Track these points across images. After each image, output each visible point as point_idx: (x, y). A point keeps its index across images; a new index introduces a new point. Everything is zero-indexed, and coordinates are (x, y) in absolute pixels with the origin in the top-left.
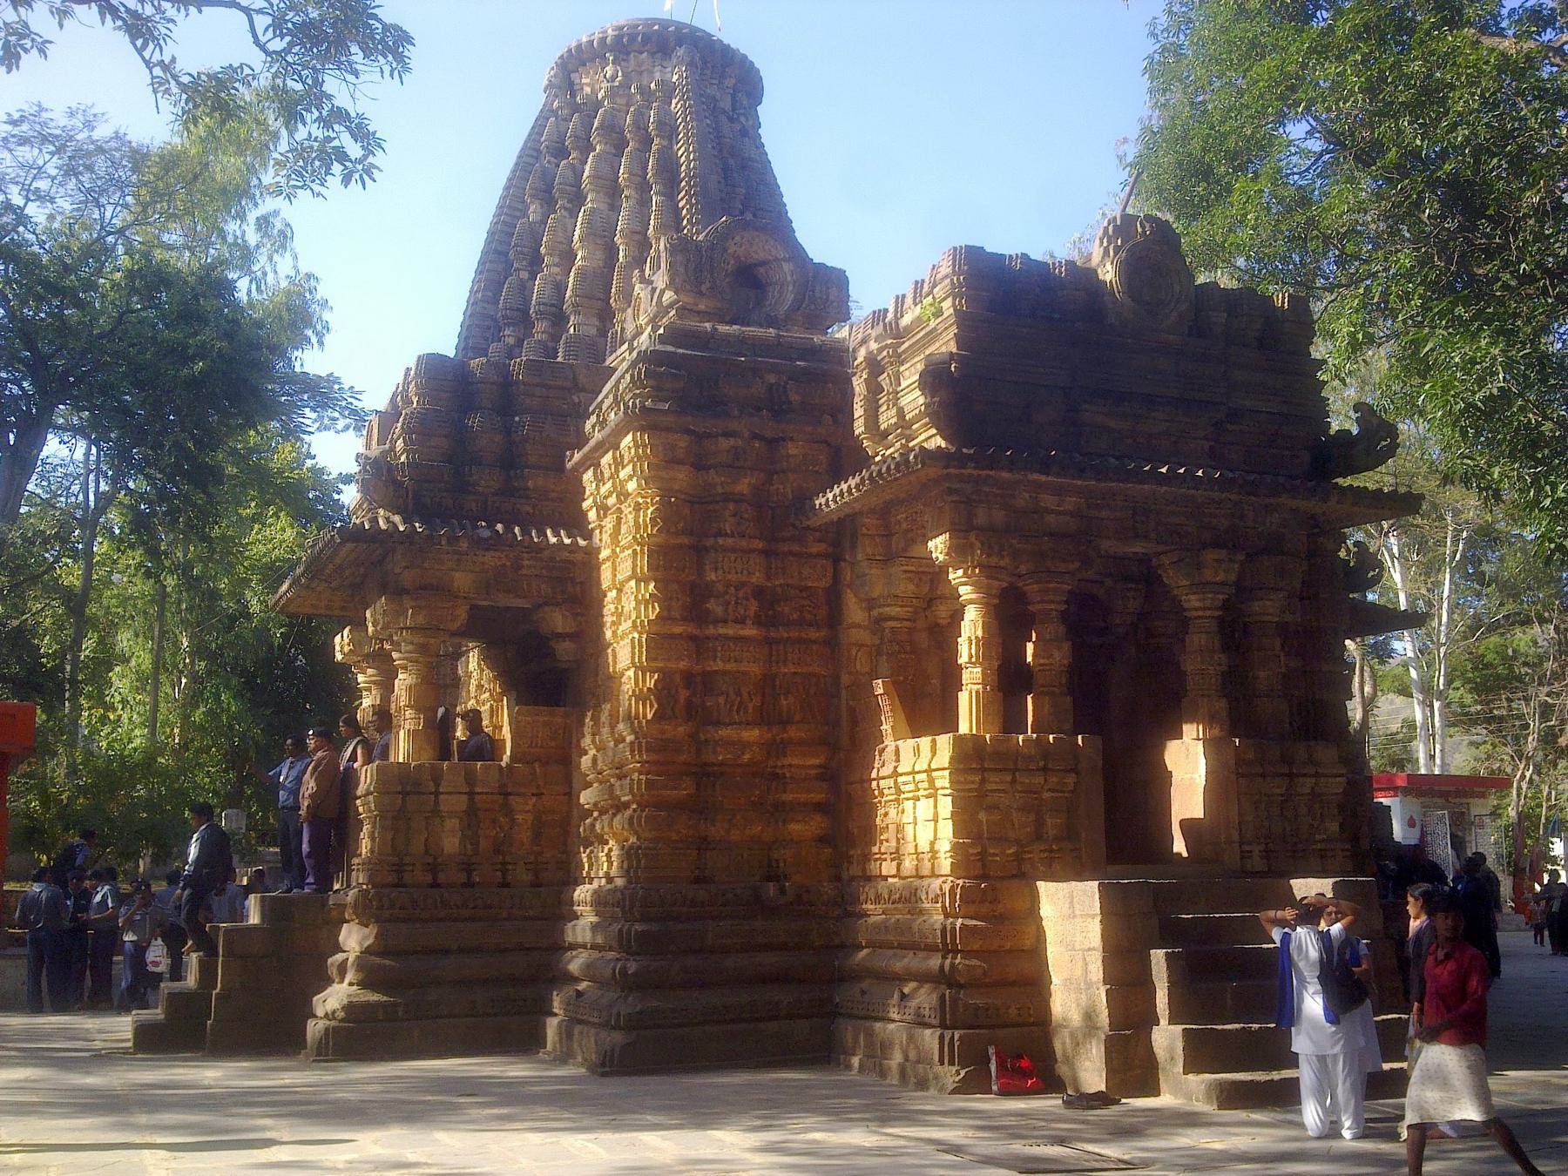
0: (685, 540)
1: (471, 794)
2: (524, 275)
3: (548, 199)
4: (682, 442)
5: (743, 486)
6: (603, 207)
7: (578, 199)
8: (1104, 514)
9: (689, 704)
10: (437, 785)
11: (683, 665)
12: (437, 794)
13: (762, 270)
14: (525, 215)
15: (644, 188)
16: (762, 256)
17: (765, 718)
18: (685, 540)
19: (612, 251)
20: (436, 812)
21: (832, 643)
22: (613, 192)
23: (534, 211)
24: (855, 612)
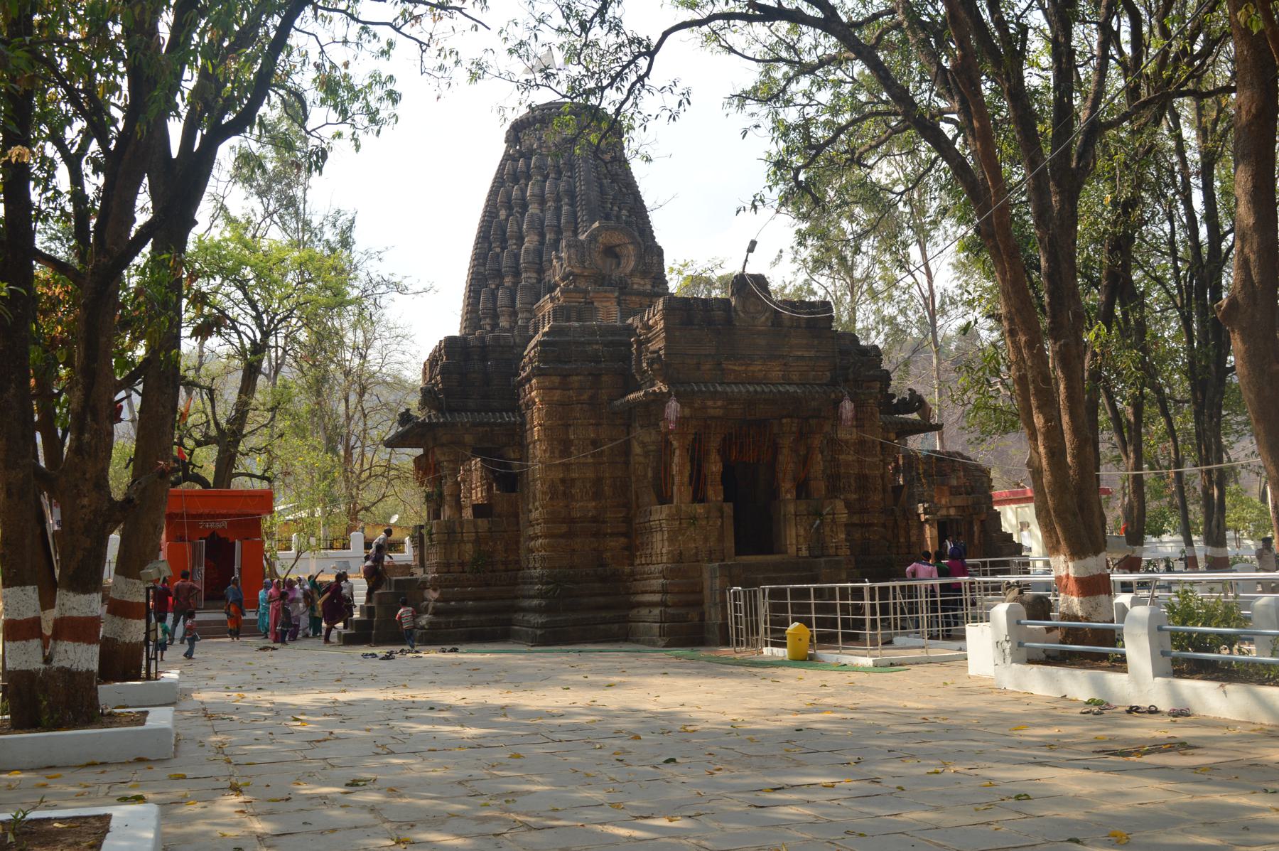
0: (560, 422)
1: (477, 532)
2: (498, 250)
3: (509, 206)
4: (557, 380)
5: (585, 397)
6: (537, 211)
7: (524, 207)
8: (735, 406)
9: (564, 494)
10: (462, 529)
11: (561, 476)
12: (462, 533)
13: (617, 249)
14: (497, 216)
15: (558, 199)
16: (617, 242)
17: (597, 495)
18: (560, 422)
19: (542, 235)
20: (462, 541)
21: (627, 463)
22: (542, 201)
23: (503, 214)
24: (637, 449)
